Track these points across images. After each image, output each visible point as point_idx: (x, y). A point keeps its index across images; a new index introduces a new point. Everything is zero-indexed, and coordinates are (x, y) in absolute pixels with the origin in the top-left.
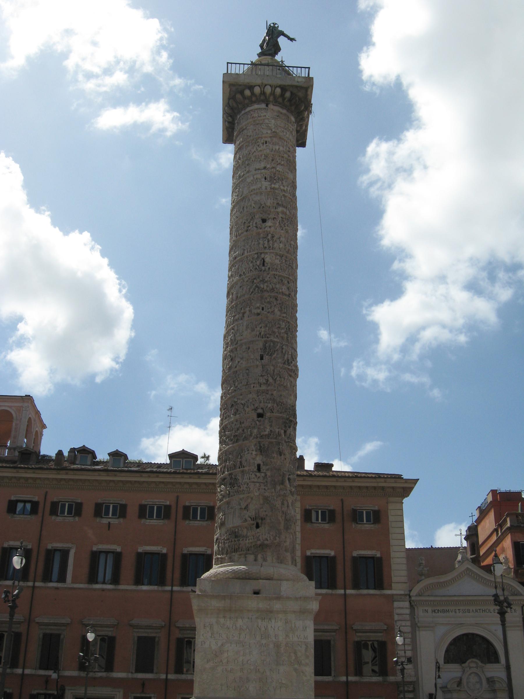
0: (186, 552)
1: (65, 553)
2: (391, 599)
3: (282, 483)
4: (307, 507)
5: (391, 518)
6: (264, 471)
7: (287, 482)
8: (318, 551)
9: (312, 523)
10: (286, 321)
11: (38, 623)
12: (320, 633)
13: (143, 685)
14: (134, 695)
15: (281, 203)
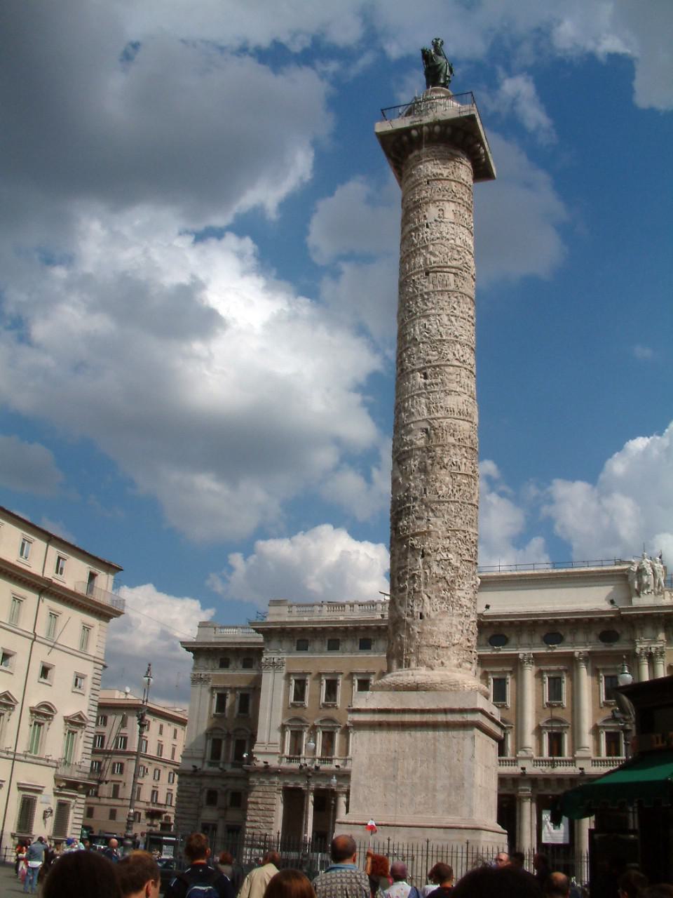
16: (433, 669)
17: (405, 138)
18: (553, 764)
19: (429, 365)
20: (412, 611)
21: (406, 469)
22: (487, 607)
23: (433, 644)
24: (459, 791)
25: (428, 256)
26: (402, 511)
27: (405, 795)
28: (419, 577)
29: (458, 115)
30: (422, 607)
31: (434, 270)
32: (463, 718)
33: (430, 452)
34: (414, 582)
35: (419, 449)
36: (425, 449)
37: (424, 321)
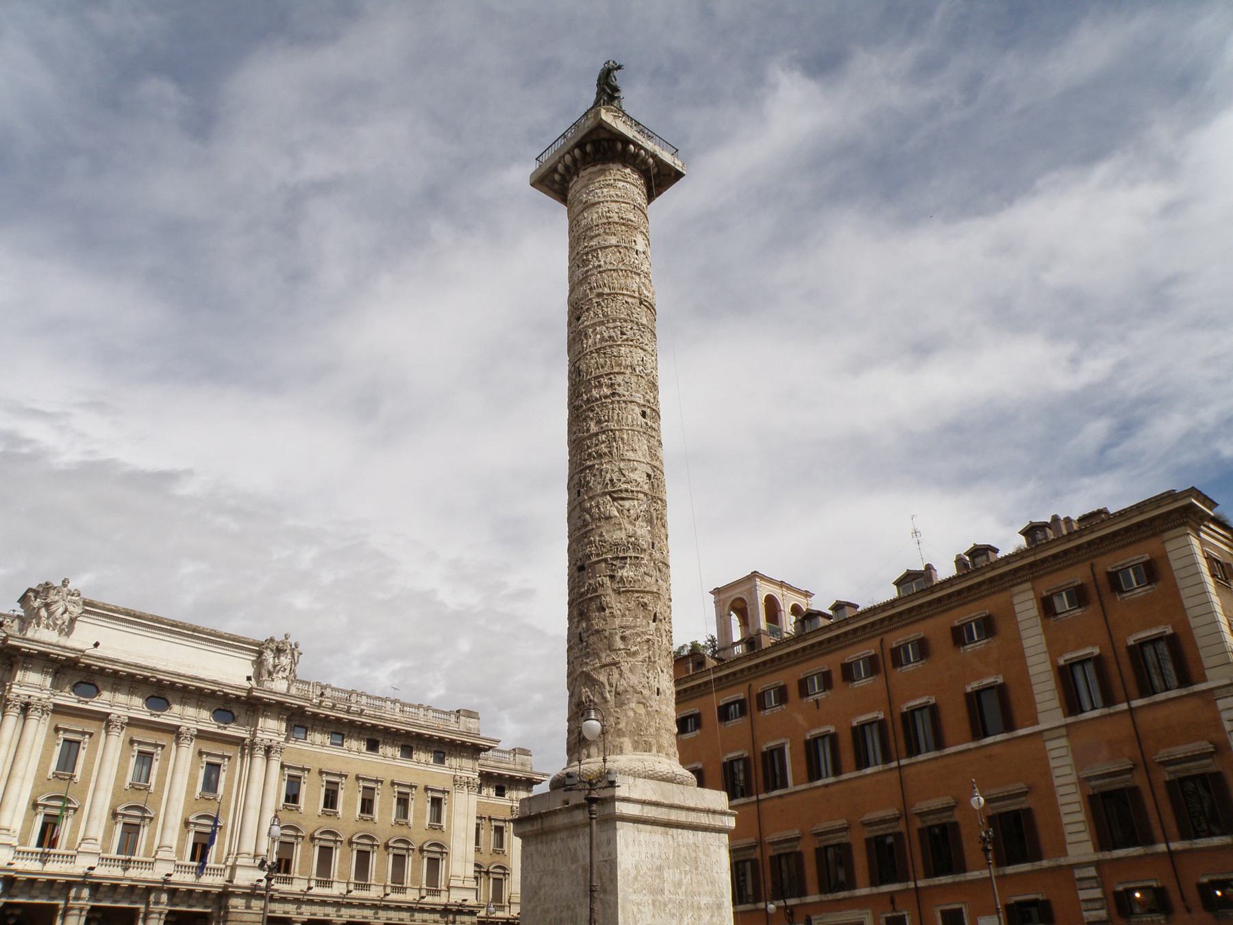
0: (905, 710)
1: (781, 750)
2: (1209, 697)
3: (610, 648)
4: (1045, 594)
5: (1175, 565)
6: (586, 639)
7: (621, 642)
8: (1074, 655)
9: (1056, 614)
10: (608, 431)
11: (770, 843)
12: (1107, 780)
13: (892, 901)
14: (884, 915)
15: (595, 285)
16: (669, 759)
17: (619, 146)
18: (126, 864)
19: (649, 405)
20: (648, 683)
21: (629, 510)
22: (96, 645)
23: (669, 727)
24: (720, 911)
25: (641, 285)
26: (626, 558)
27: (673, 915)
28: (653, 644)
29: (673, 165)
30: (659, 682)
31: (646, 303)
32: (722, 822)
33: (655, 502)
34: (649, 650)
35: (646, 494)
36: (650, 497)
37: (642, 353)
